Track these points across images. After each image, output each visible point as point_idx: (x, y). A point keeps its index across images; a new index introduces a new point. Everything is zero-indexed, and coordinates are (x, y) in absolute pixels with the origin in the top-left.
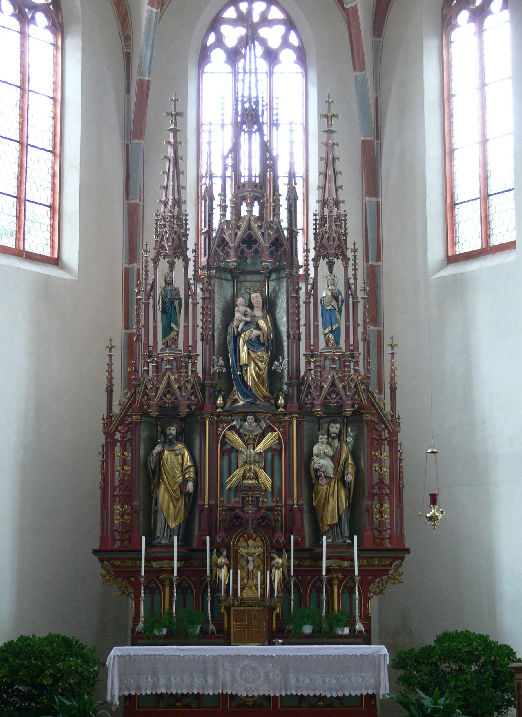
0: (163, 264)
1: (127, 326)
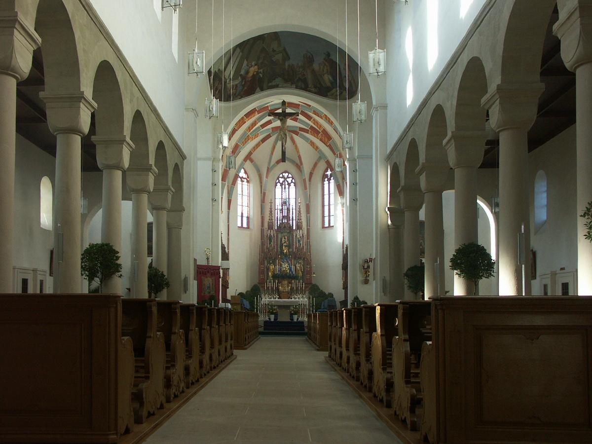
0: (269, 231)
1: (261, 240)
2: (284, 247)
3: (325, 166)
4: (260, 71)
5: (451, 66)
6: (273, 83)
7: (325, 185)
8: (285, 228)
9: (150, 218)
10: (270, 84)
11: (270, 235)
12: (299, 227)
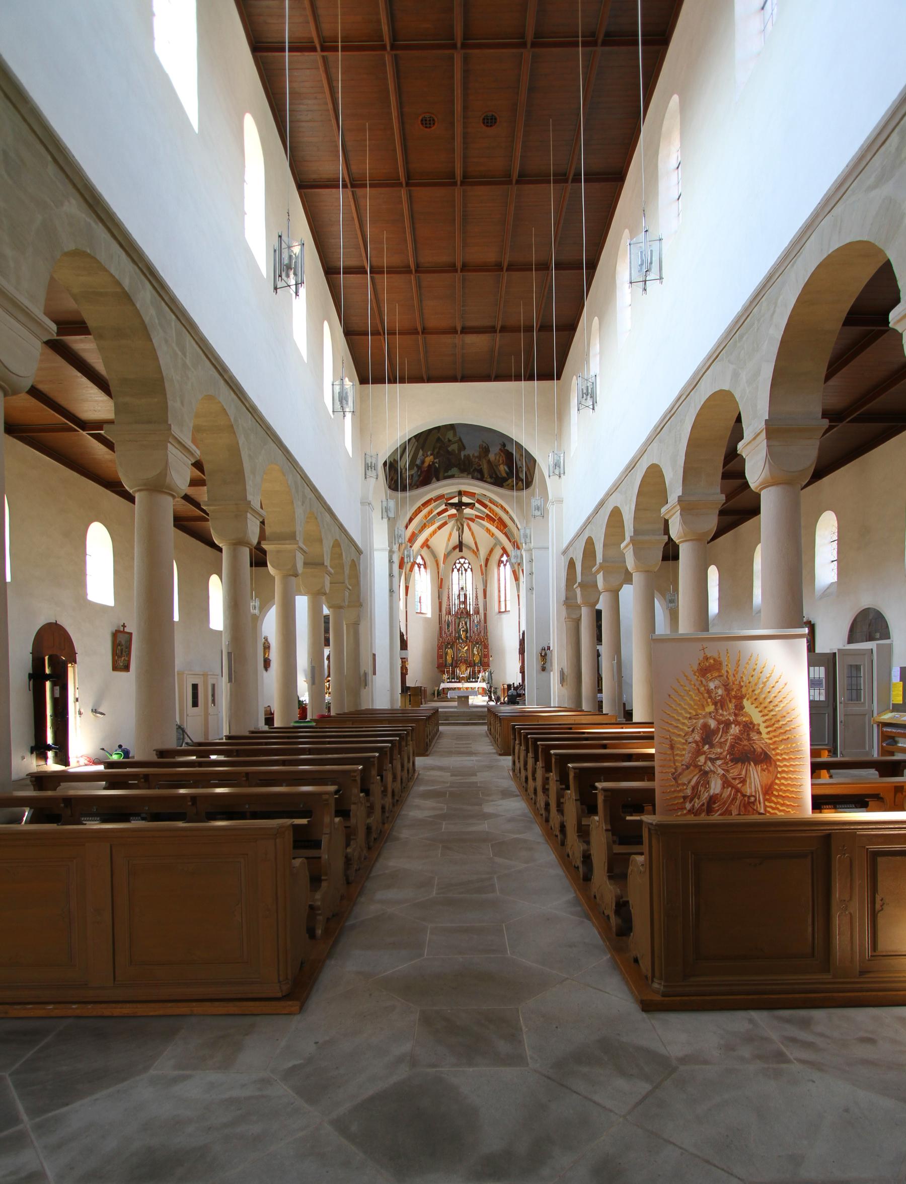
0: (447, 616)
2: (461, 632)
3: (501, 552)
4: (435, 461)
5: (630, 469)
6: (450, 473)
7: (501, 571)
8: (464, 614)
9: (326, 611)
10: (446, 474)
11: (448, 620)
12: (477, 612)
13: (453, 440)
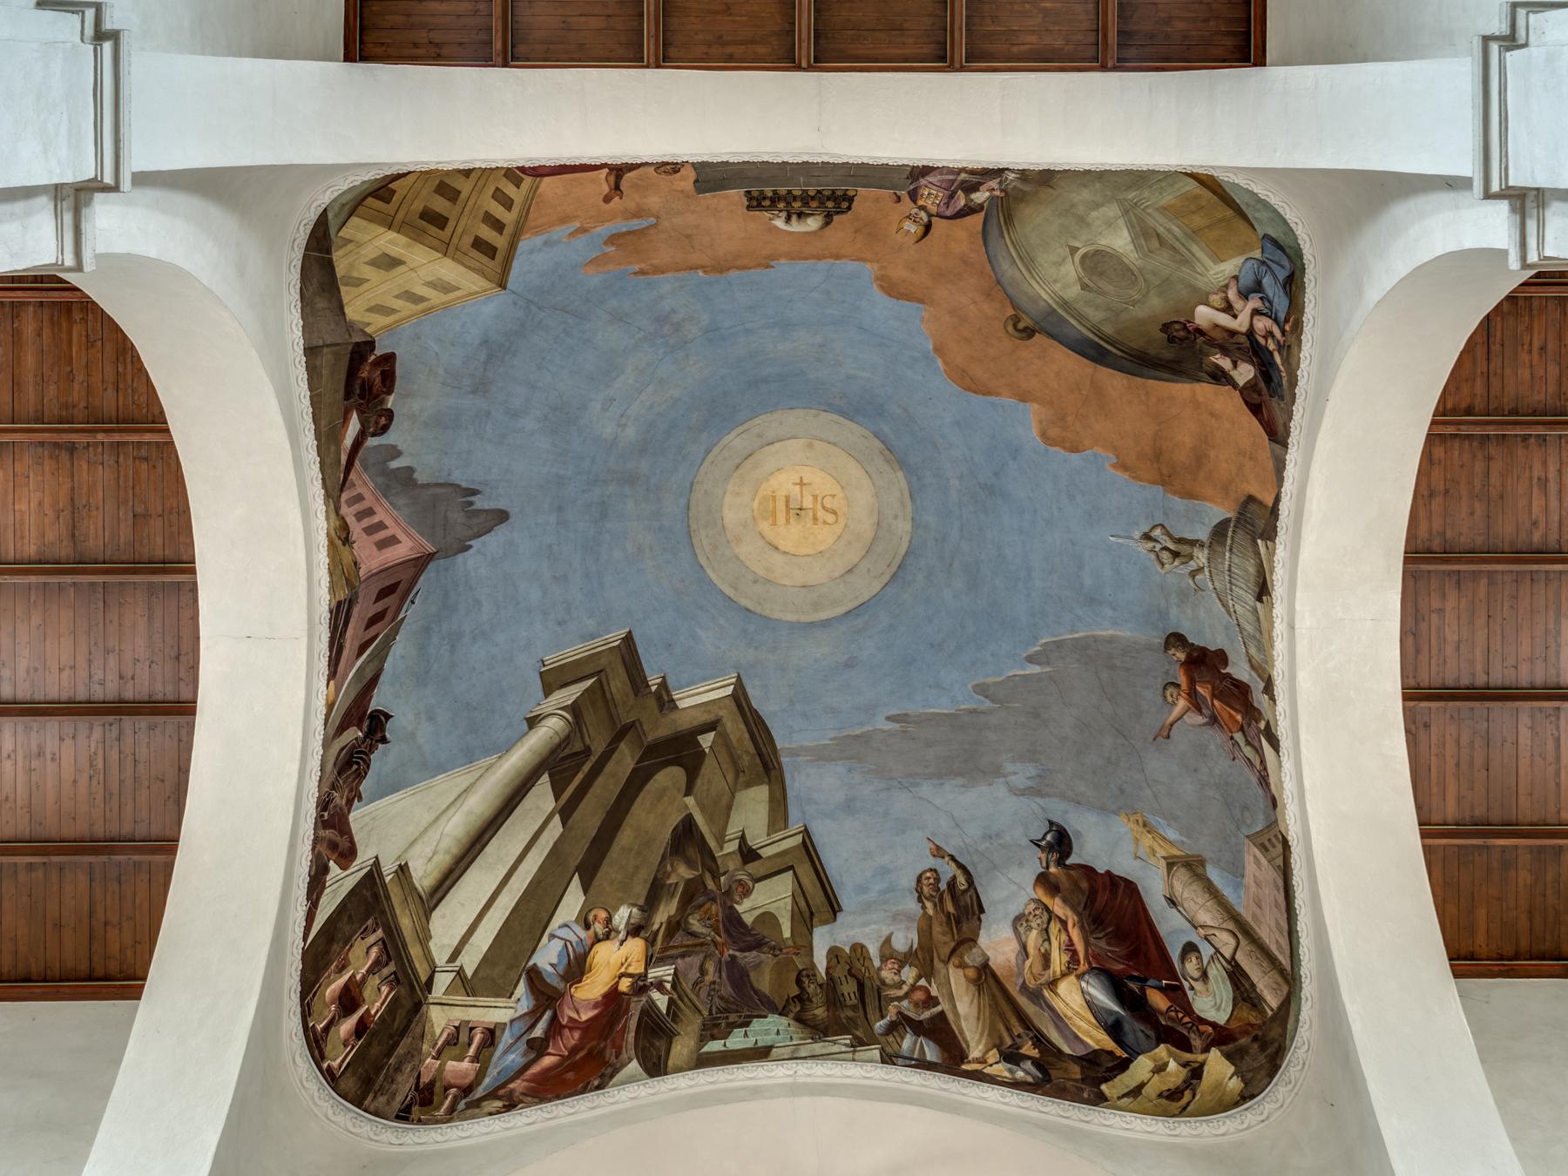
6: (736, 1041)
10: (715, 1046)
13: (765, 853)
